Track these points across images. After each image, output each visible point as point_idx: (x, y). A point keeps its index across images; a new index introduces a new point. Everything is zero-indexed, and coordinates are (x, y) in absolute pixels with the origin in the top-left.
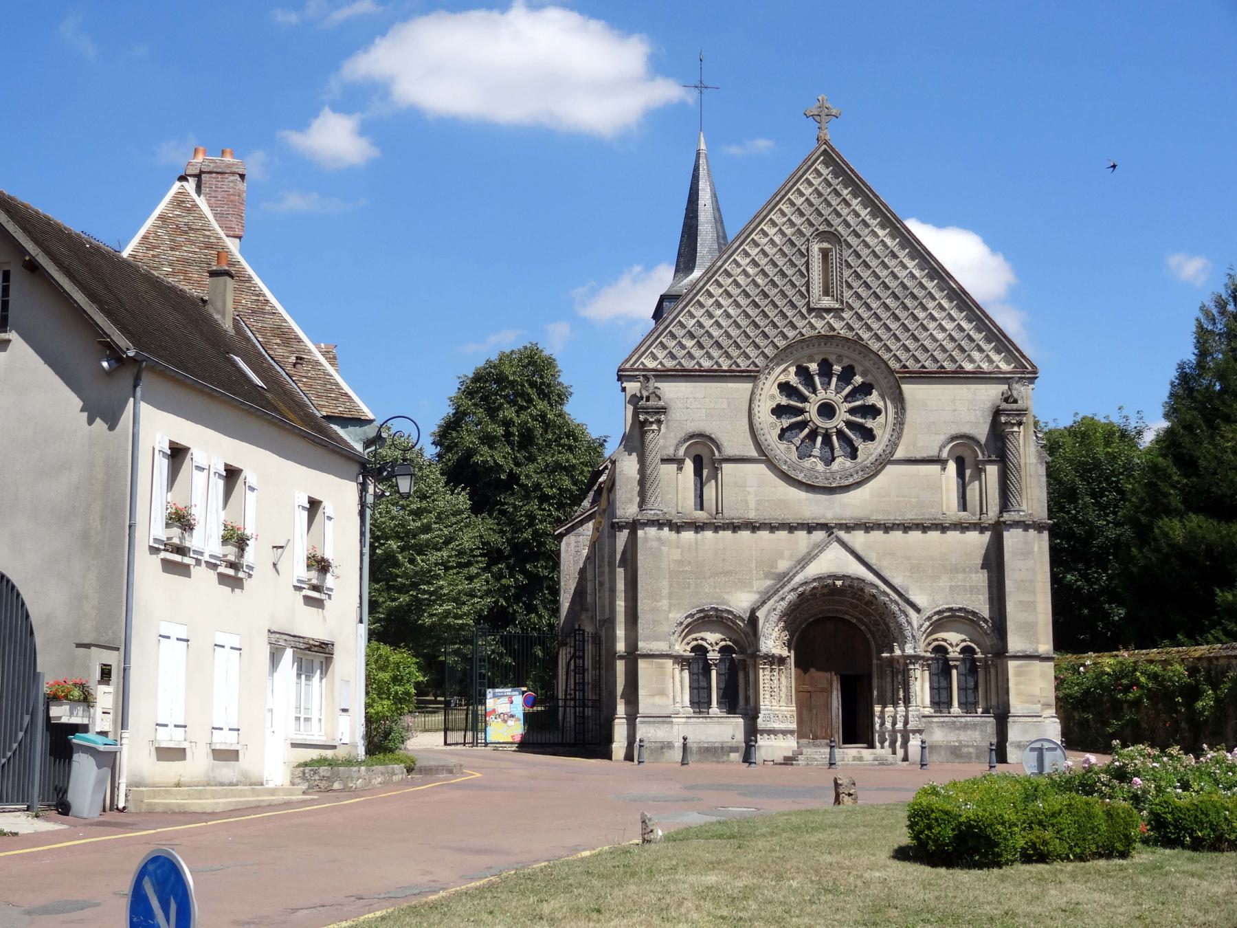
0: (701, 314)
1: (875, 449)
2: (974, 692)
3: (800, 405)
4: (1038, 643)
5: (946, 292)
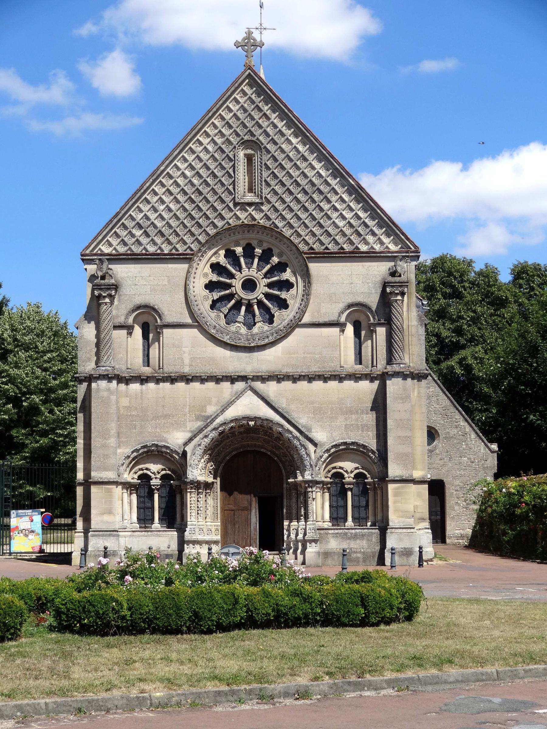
0: (147, 209)
1: (288, 316)
2: (365, 510)
3: (228, 281)
4: (414, 468)
5: (346, 188)
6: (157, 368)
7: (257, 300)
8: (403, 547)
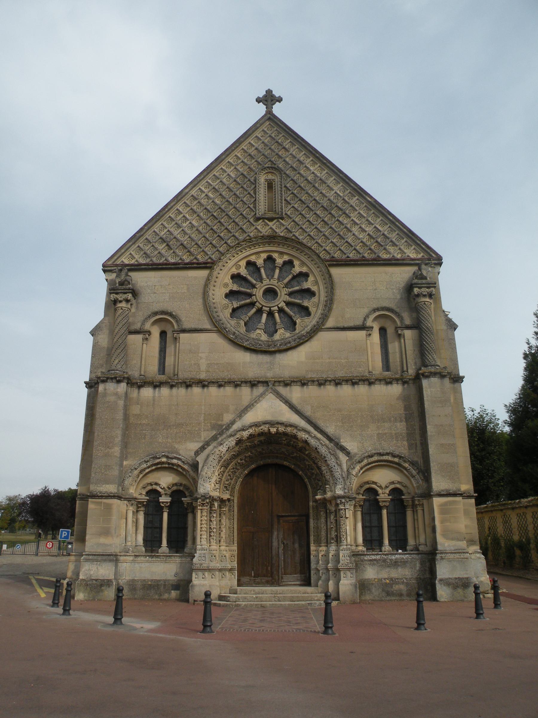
6: (172, 375)
7: (278, 307)
8: (457, 577)
